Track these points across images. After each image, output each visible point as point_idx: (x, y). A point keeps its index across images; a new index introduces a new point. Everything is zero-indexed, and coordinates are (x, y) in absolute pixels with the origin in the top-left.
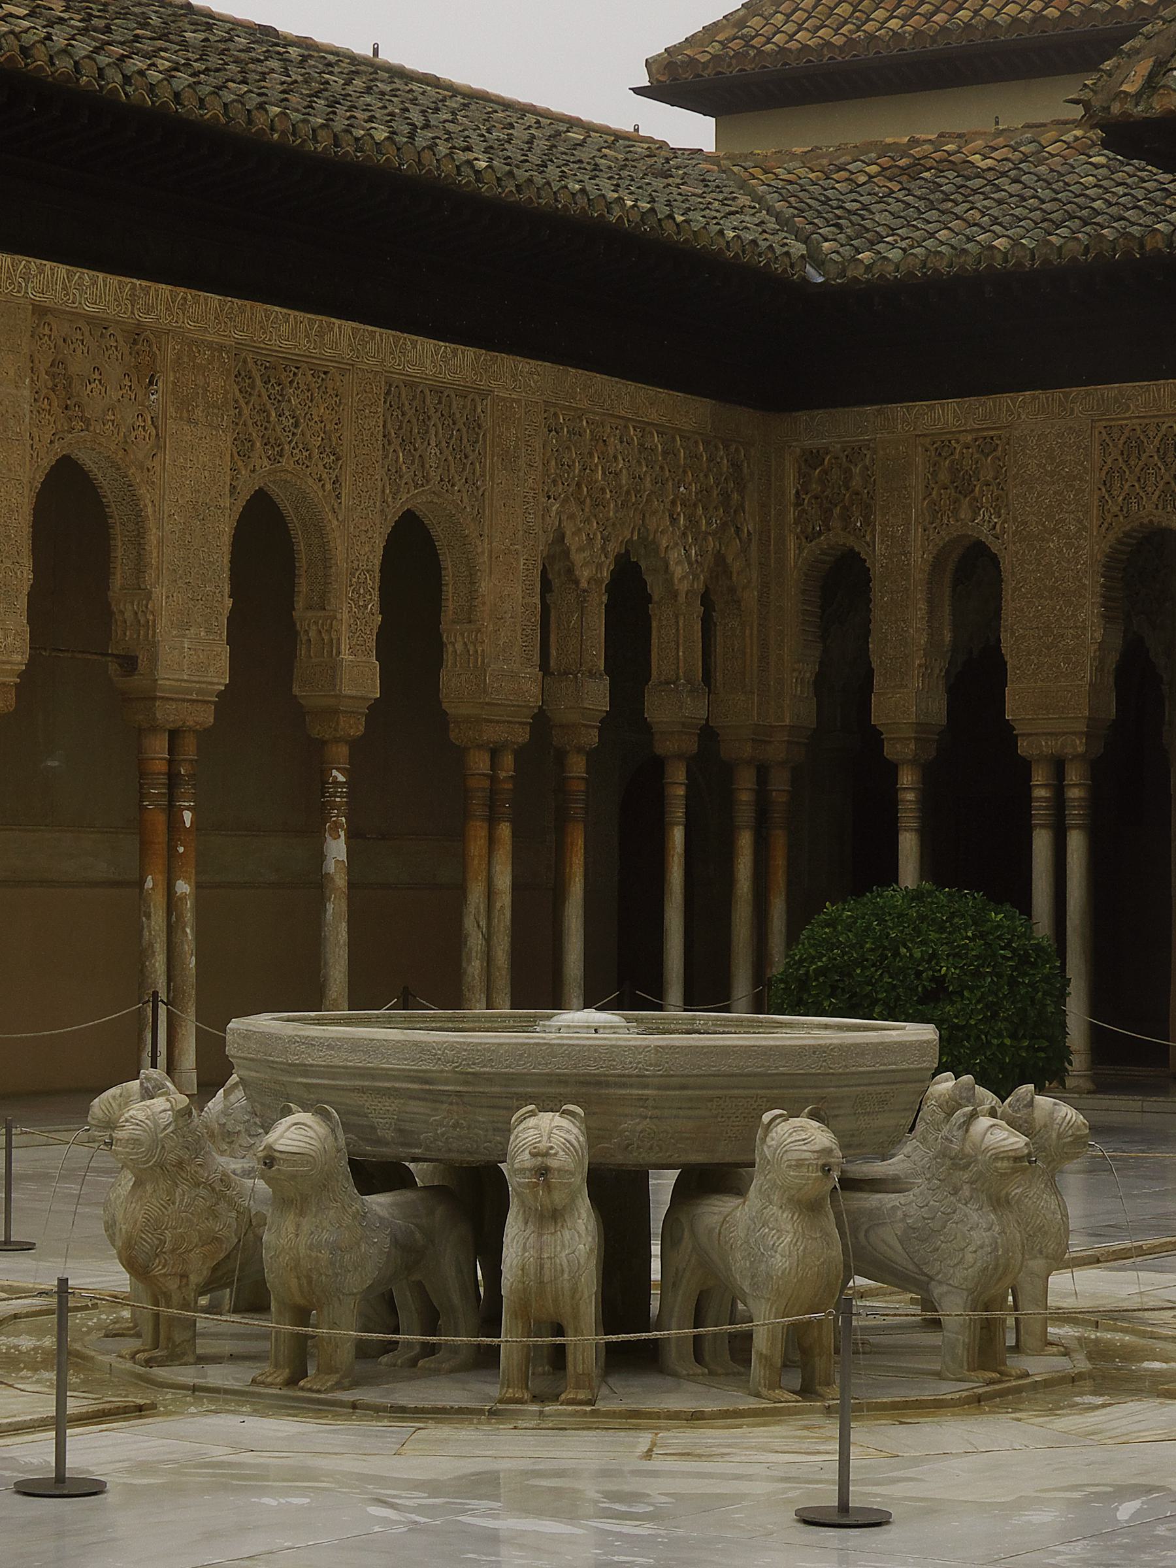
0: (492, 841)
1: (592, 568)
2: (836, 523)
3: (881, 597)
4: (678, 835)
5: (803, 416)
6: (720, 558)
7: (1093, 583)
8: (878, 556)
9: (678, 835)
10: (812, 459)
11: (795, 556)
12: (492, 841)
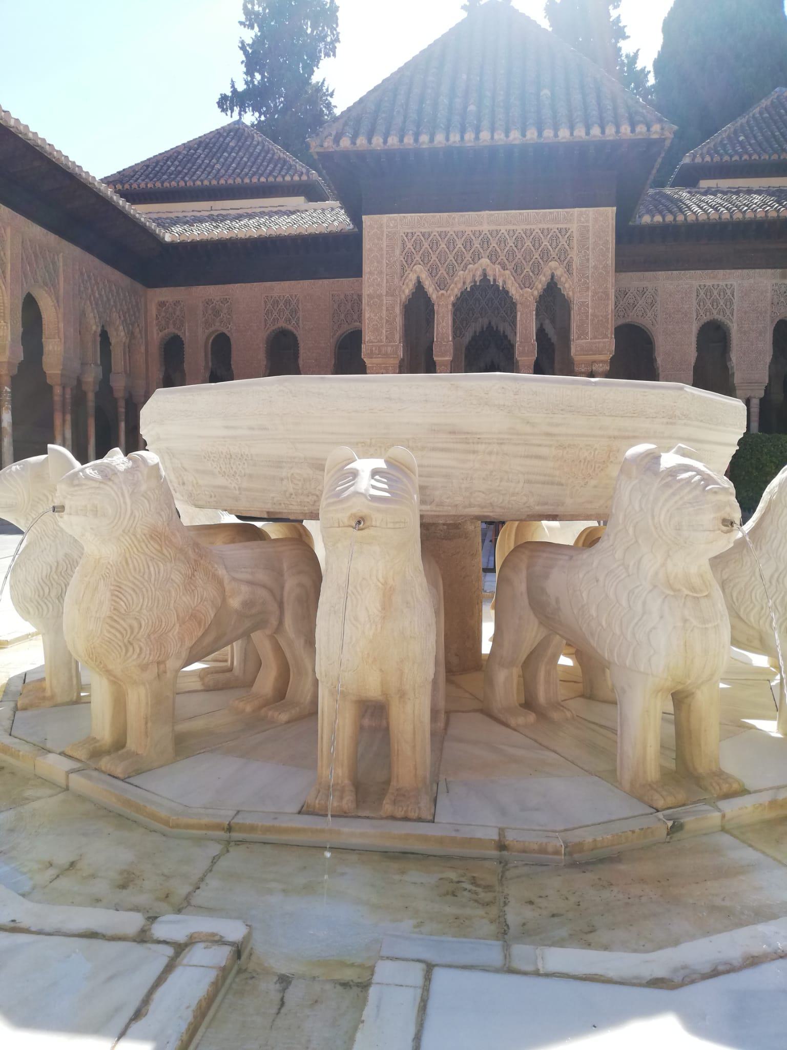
0: (64, 421)
1: (95, 328)
2: (171, 326)
3: (188, 350)
4: (123, 425)
5: (158, 290)
6: (132, 333)
7: (262, 346)
8: (186, 337)
9: (123, 425)
10: (162, 304)
11: (156, 336)
12: (64, 421)
